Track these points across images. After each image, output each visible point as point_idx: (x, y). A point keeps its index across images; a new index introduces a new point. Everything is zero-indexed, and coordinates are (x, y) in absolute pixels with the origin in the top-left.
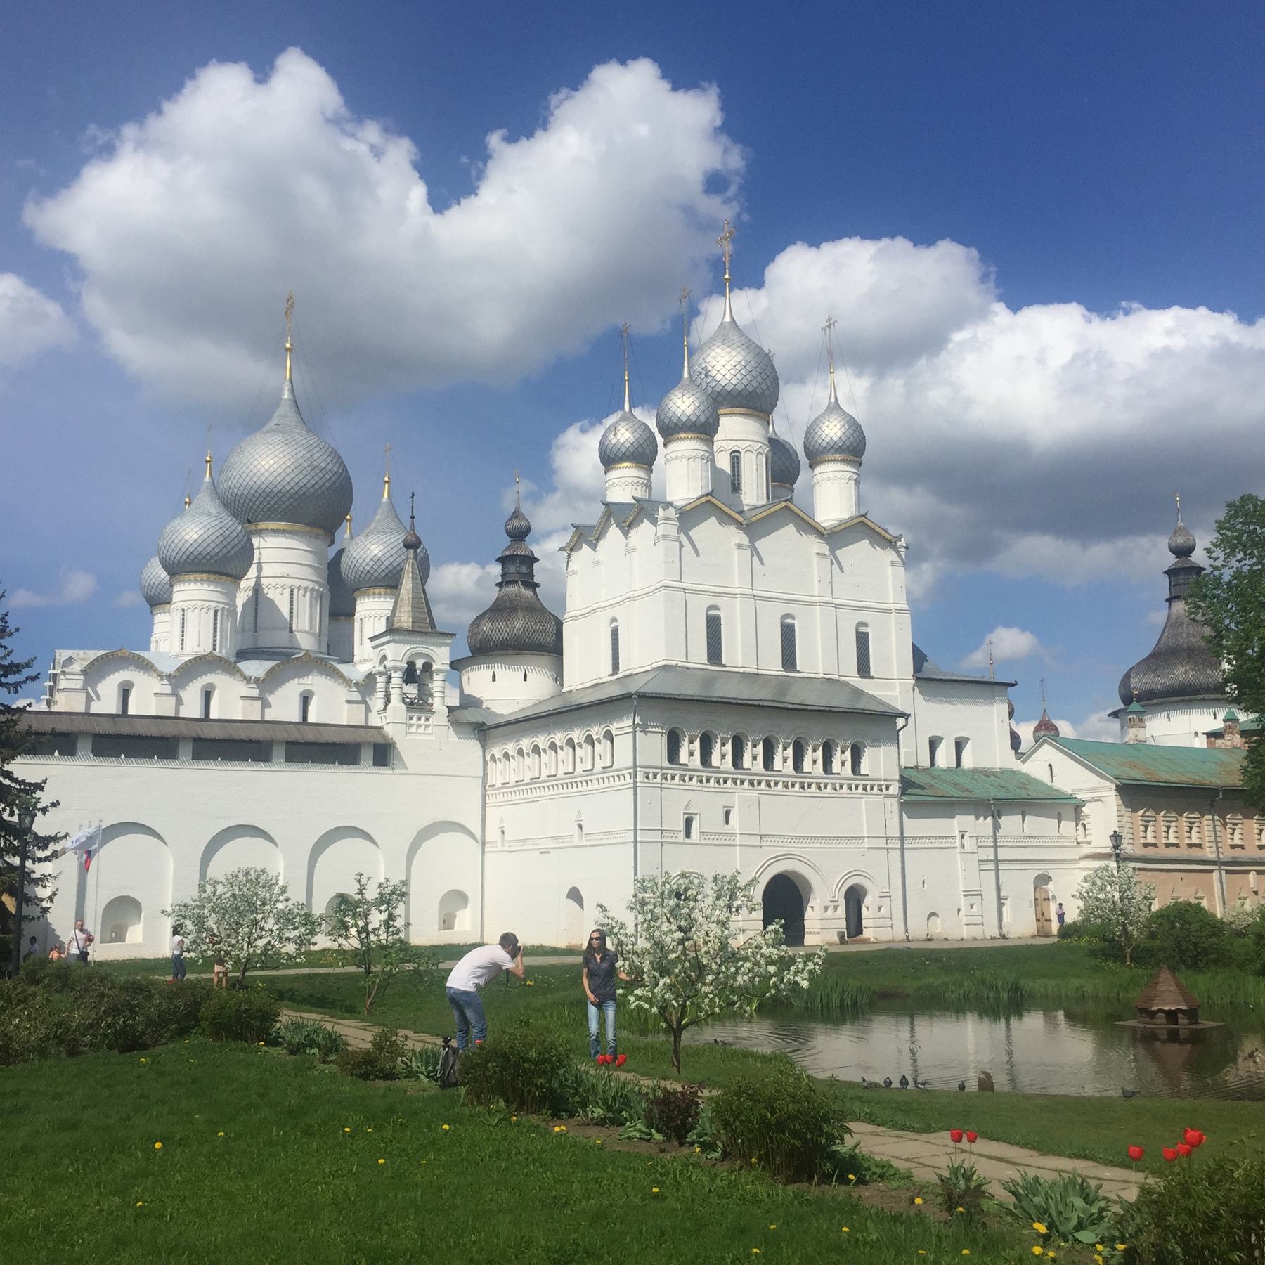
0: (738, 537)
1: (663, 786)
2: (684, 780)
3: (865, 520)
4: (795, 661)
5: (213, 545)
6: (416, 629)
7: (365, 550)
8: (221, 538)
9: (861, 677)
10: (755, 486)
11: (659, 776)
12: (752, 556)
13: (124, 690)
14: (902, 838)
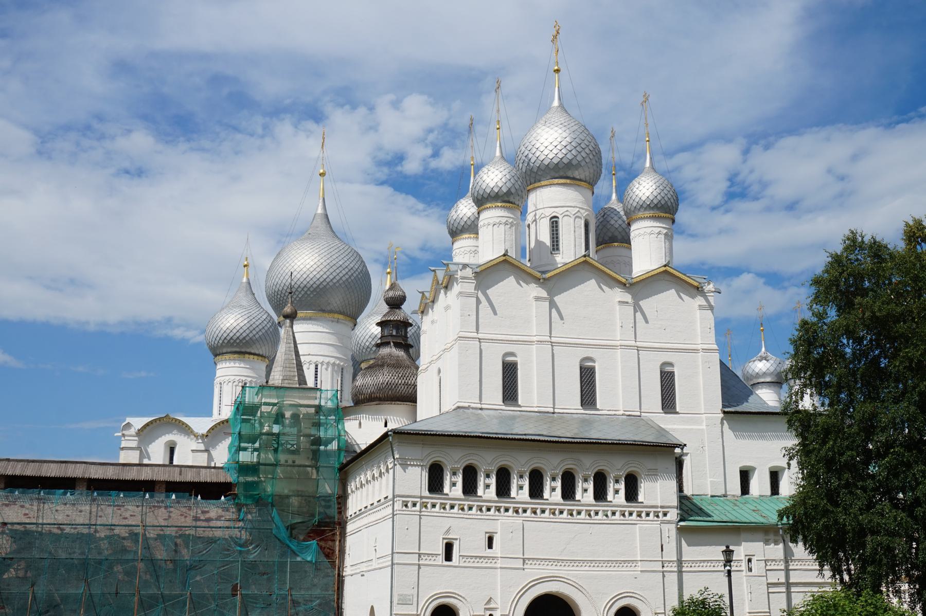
0: (534, 290)
1: (422, 513)
2: (572, 515)
3: (668, 268)
4: (675, 403)
5: (241, 331)
6: (283, 385)
7: (365, 329)
8: (248, 325)
9: (665, 413)
10: (573, 246)
11: (418, 505)
12: (635, 311)
13: (171, 448)
14: (680, 562)
